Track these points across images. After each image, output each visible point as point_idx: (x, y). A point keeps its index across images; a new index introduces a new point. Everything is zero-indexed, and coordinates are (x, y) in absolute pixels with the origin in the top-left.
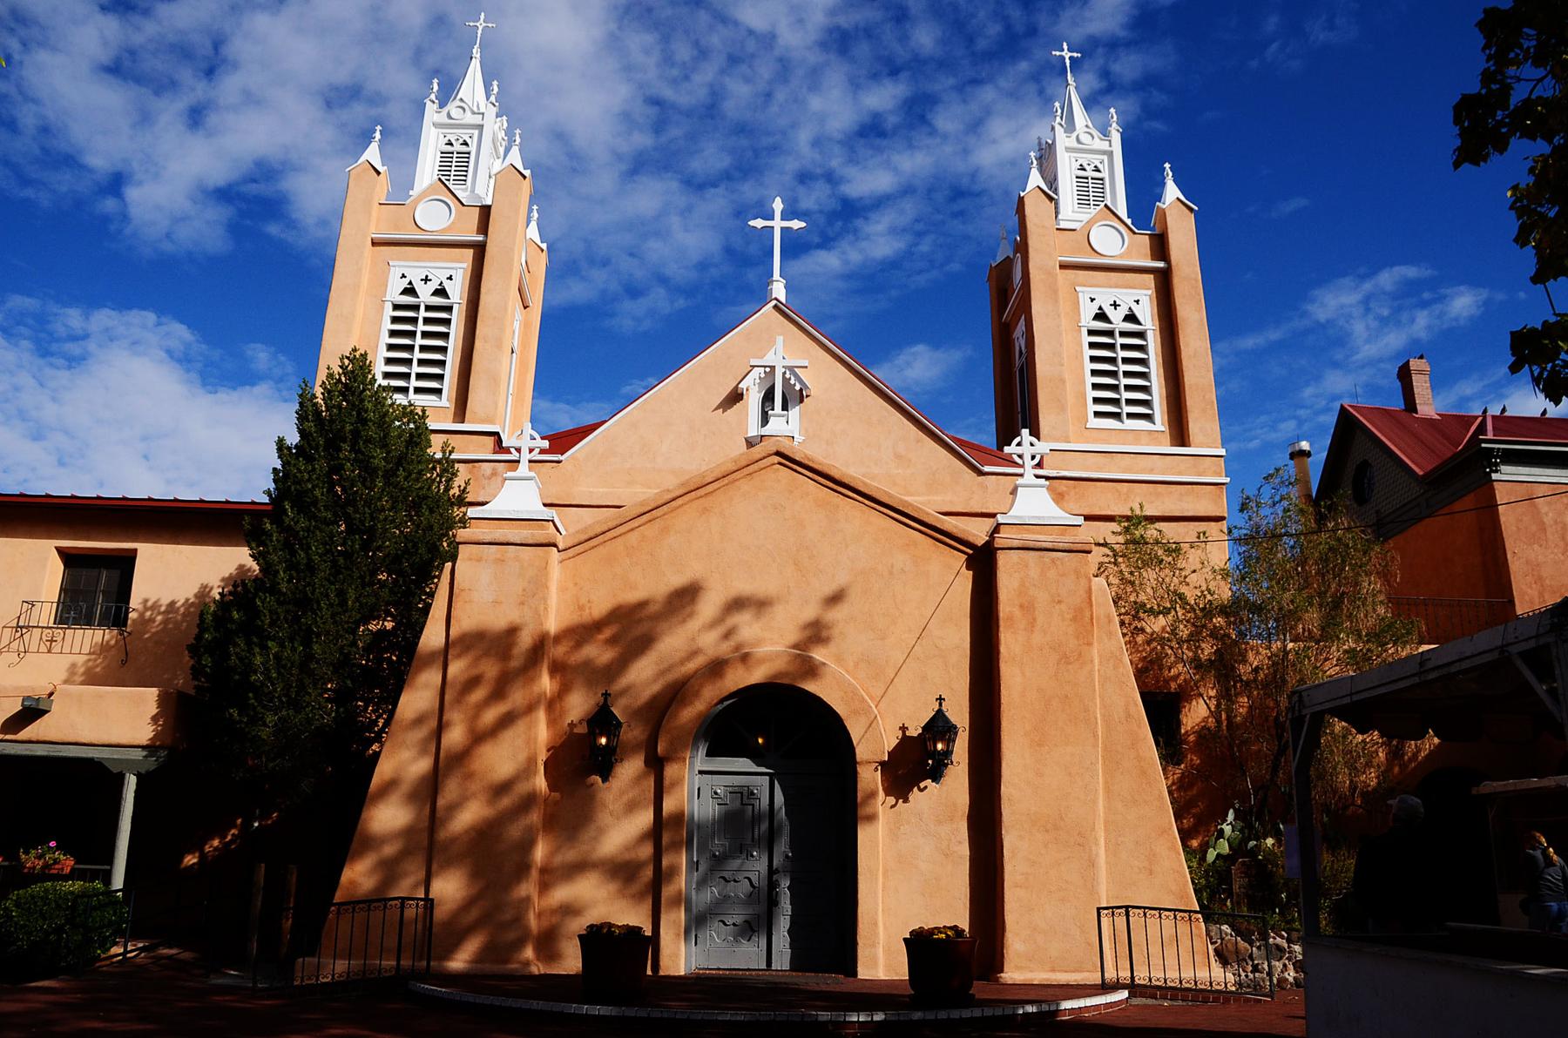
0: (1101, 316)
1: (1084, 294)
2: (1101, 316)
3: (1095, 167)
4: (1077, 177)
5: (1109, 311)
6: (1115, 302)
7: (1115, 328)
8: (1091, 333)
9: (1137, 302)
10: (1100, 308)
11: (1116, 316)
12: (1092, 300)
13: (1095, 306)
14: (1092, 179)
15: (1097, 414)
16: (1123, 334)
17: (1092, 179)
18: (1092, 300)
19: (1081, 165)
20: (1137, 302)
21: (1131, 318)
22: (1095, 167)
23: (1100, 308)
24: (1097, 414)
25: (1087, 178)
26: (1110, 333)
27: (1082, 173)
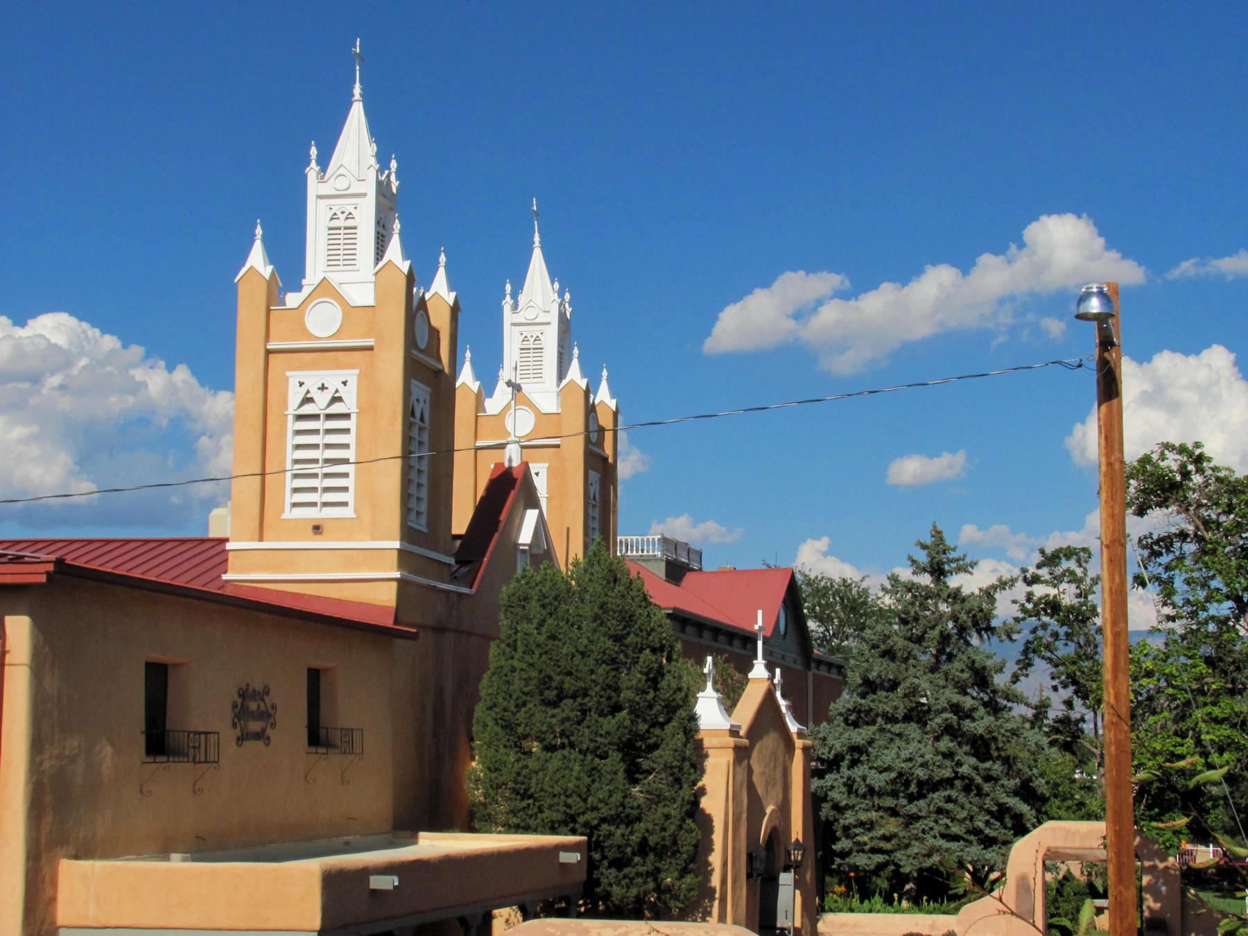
1: (294, 377)
2: (307, 400)
3: (350, 214)
5: (315, 394)
6: (323, 385)
8: (300, 418)
9: (345, 383)
12: (301, 384)
13: (304, 389)
14: (345, 228)
16: (329, 417)
17: (345, 228)
18: (301, 384)
19: (335, 214)
20: (345, 383)
22: (350, 214)
23: (308, 392)
24: (295, 505)
26: (315, 417)
27: (335, 223)
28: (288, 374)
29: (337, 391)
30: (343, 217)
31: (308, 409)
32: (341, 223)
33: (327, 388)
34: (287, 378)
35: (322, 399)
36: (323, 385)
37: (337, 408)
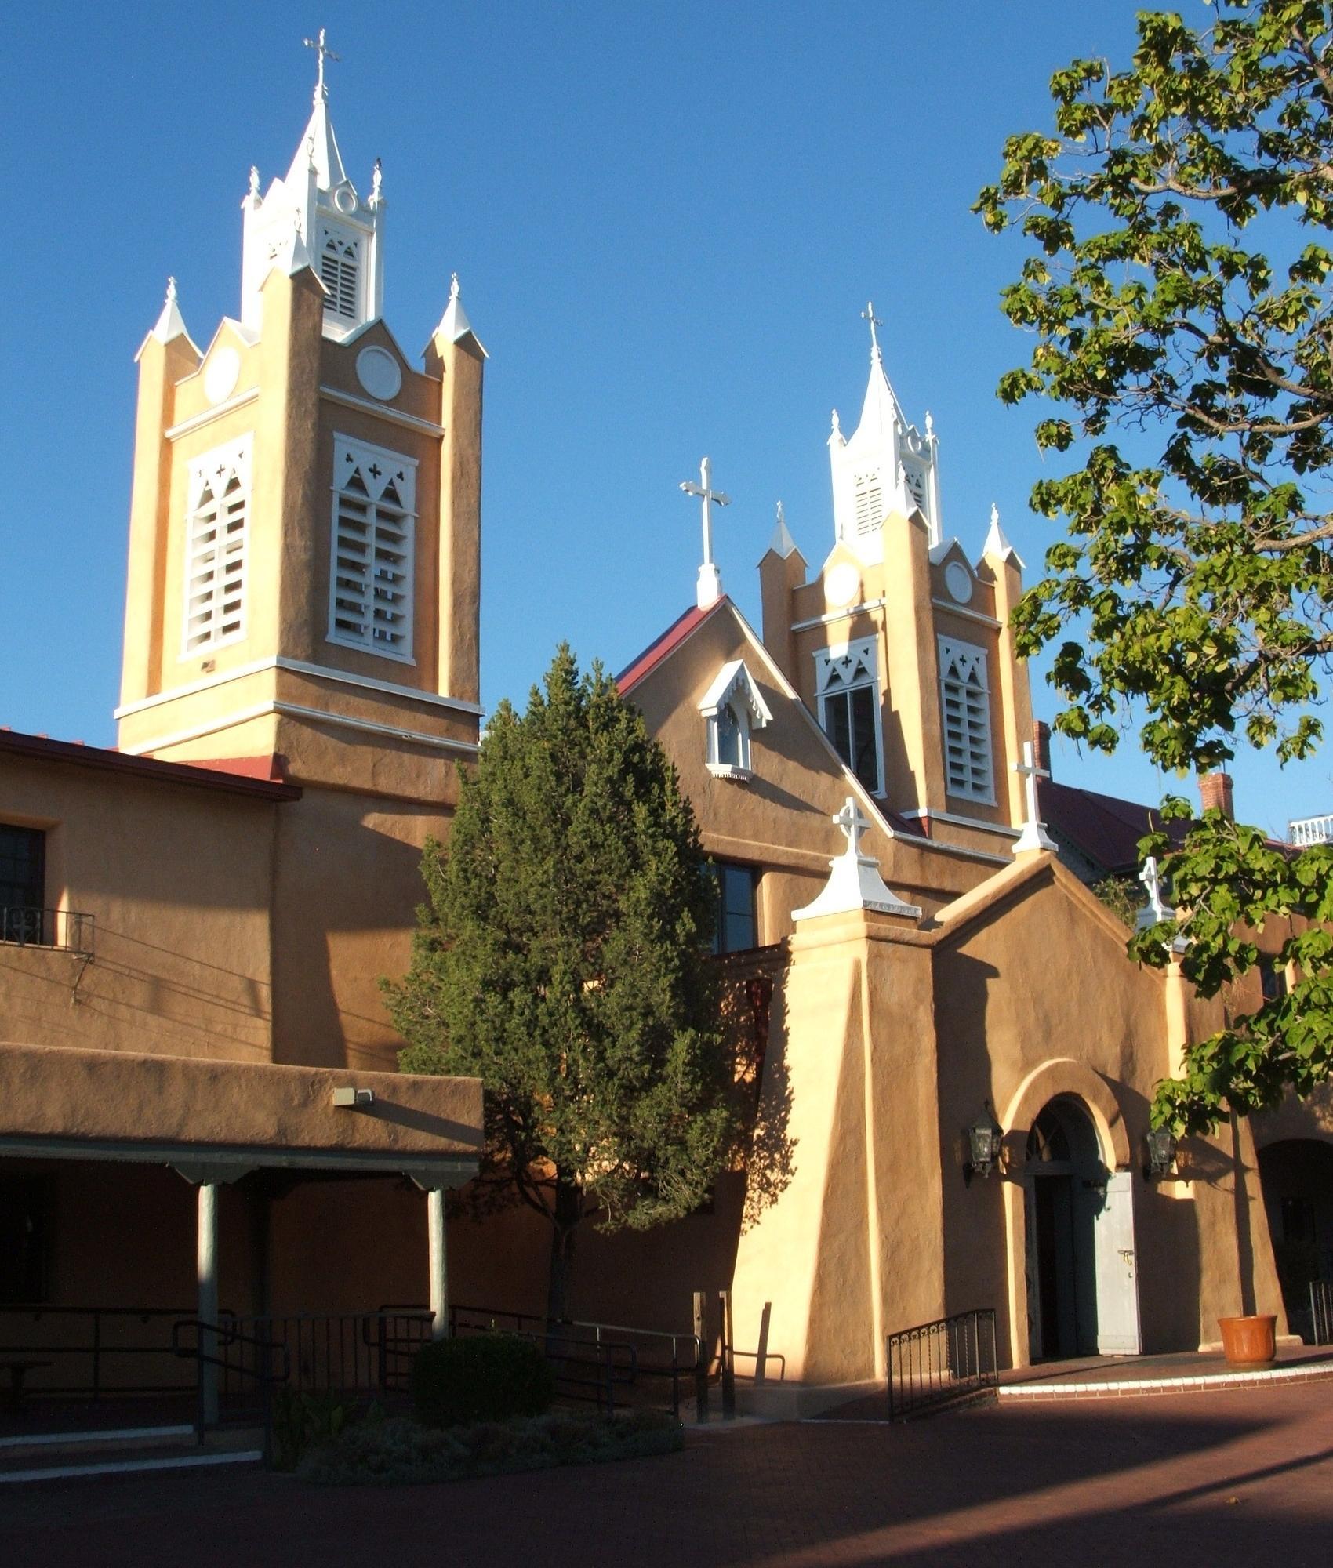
0: (356, 483)
2: (356, 483)
4: (324, 257)
5: (367, 478)
6: (375, 466)
7: (371, 504)
8: (345, 503)
10: (357, 471)
11: (375, 488)
12: (349, 459)
13: (352, 467)
15: (342, 624)
16: (381, 514)
21: (391, 495)
23: (357, 471)
25: (336, 262)
26: (362, 508)
27: (331, 254)
28: (336, 435)
29: (391, 483)
30: (341, 249)
31: (355, 495)
32: (340, 257)
33: (379, 473)
34: (333, 440)
35: (375, 488)
36: (375, 466)
37: (390, 507)
